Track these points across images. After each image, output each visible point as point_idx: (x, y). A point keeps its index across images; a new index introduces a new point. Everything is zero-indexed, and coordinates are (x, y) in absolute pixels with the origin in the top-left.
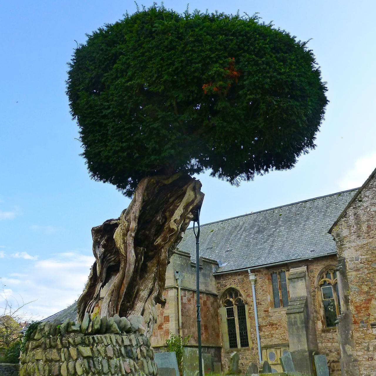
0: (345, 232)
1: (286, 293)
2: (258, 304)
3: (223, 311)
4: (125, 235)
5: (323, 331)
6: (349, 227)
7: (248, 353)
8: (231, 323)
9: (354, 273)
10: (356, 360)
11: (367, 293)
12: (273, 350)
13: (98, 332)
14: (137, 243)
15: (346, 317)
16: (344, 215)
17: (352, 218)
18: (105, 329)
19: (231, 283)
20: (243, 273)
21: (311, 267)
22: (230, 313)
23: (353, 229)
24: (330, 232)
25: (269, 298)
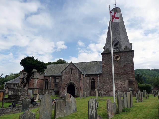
1: (56, 81)
2: (51, 82)
3: (45, 83)
4: (25, 80)
6: (64, 73)
12: (52, 90)
14: (26, 80)
16: (64, 71)
17: (64, 72)
18: (22, 89)
20: (49, 76)
22: (46, 83)
25: (53, 81)
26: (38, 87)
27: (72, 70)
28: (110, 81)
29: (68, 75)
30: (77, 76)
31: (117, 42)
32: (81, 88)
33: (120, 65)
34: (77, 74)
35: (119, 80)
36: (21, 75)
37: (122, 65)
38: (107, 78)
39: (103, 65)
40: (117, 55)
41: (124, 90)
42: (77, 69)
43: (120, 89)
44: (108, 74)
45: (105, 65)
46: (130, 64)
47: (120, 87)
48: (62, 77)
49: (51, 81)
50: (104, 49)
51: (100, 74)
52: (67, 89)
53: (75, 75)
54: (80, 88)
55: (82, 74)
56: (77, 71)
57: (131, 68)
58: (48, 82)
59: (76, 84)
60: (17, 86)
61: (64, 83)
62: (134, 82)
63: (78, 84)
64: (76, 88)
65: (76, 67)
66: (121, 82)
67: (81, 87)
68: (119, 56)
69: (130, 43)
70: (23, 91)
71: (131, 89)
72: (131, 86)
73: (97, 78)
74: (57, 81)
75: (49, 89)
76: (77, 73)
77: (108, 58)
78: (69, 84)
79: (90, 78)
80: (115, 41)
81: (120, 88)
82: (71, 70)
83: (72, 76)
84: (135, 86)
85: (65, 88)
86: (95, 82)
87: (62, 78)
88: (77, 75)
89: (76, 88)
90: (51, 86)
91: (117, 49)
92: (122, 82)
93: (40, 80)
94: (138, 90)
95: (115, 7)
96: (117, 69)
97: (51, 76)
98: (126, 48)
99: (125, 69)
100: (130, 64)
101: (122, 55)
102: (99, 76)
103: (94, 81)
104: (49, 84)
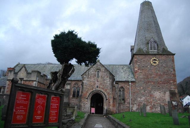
5: (72, 98)
6: (86, 76)
10: (81, 106)
15: (81, 96)
16: (86, 72)
21: (72, 82)
23: (87, 76)
24: (81, 76)
29: (92, 79)
30: (108, 81)
32: (115, 100)
33: (159, 71)
34: (108, 78)
36: (9, 74)
38: (142, 88)
40: (154, 58)
43: (159, 103)
45: (138, 70)
48: (84, 82)
51: (131, 82)
52: (90, 100)
53: (104, 80)
61: (87, 92)
63: (109, 93)
66: (159, 94)
67: (115, 98)
68: (157, 60)
71: (175, 103)
81: (159, 102)
83: (99, 80)
85: (87, 99)
86: (125, 92)
87: (83, 83)
91: (155, 50)
92: (162, 94)
99: (165, 77)
101: (161, 58)
102: (130, 84)
103: (124, 90)
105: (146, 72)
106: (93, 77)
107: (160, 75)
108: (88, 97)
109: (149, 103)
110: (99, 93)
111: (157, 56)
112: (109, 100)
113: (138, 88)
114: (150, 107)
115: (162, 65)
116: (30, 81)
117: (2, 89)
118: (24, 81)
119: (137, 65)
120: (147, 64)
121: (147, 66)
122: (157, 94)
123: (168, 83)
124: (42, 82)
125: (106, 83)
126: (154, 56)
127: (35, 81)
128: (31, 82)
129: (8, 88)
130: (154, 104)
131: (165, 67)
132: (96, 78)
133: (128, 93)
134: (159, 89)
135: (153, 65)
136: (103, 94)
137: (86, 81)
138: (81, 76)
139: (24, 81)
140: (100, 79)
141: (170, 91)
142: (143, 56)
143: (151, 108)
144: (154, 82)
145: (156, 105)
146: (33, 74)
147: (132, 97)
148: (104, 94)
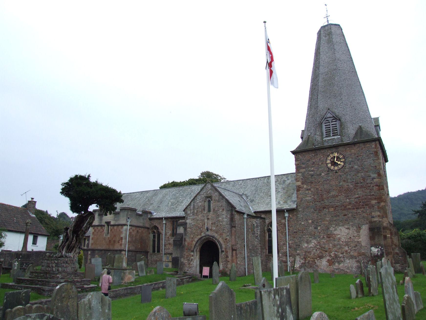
0: (189, 212)
3: (151, 236)
4: (70, 232)
6: (190, 210)
7: (159, 255)
8: (154, 241)
9: (189, 229)
10: (184, 264)
11: (192, 238)
12: (168, 255)
13: (59, 257)
16: (190, 204)
19: (156, 223)
20: (161, 219)
22: (154, 237)
23: (192, 211)
25: (170, 232)
26: (132, 248)
27: (212, 202)
28: (319, 228)
29: (200, 217)
30: (225, 218)
31: (334, 117)
33: (344, 181)
34: (224, 212)
35: (343, 226)
37: (349, 181)
38: (310, 221)
39: (299, 183)
41: (359, 253)
42: (223, 197)
43: (346, 251)
44: (312, 210)
45: (302, 184)
46: (373, 179)
47: (347, 244)
48: (188, 221)
49: (165, 231)
50: (302, 138)
51: (289, 211)
52: (198, 253)
53: (218, 216)
54: (231, 251)
55: (238, 212)
56: (224, 203)
57: (375, 188)
58: (159, 234)
59: (220, 240)
60: (86, 244)
61: (192, 240)
62: (385, 228)
63: (226, 239)
64: (222, 251)
65: (220, 194)
66: (347, 231)
69: (373, 115)
70: (64, 263)
71: (376, 250)
72: (376, 240)
73: (283, 221)
74: (181, 230)
75: (162, 250)
76: (223, 210)
77: (310, 163)
78: (204, 239)
79: (265, 222)
80: (329, 115)
81: (346, 248)
82: (209, 201)
83: (210, 217)
84: (389, 240)
85: (193, 251)
88: (224, 216)
89: (222, 251)
90: (165, 246)
91: (336, 137)
92: (352, 232)
93: (138, 229)
94: (398, 251)
95: (326, 24)
96: (337, 194)
97: (166, 218)
98: (359, 131)
99: (360, 192)
100: (373, 179)
102: (286, 215)
104: (162, 240)
105: (317, 187)
106: (200, 213)
107: (348, 190)
108: (194, 248)
109: (326, 251)
110: (211, 240)
111: (341, 149)
112: (227, 252)
113: (303, 223)
114: (328, 261)
115: (352, 167)
116: (118, 225)
117: (86, 240)
118: (111, 226)
119: (300, 174)
120: (320, 169)
121: (321, 174)
122: (342, 232)
123: (366, 205)
124: (141, 225)
125: (222, 222)
126: (334, 150)
127: (125, 225)
128: (120, 227)
129: (92, 239)
130: (336, 255)
131: (358, 172)
132: (205, 213)
133: (284, 234)
134: (345, 222)
135: (332, 170)
136: (216, 241)
137: (190, 220)
138: (184, 211)
139: (111, 226)
140: (211, 214)
141: (371, 222)
142: (312, 155)
143: (331, 263)
144: (335, 207)
145: (341, 255)
146: (121, 214)
147: (290, 242)
148: (219, 241)
